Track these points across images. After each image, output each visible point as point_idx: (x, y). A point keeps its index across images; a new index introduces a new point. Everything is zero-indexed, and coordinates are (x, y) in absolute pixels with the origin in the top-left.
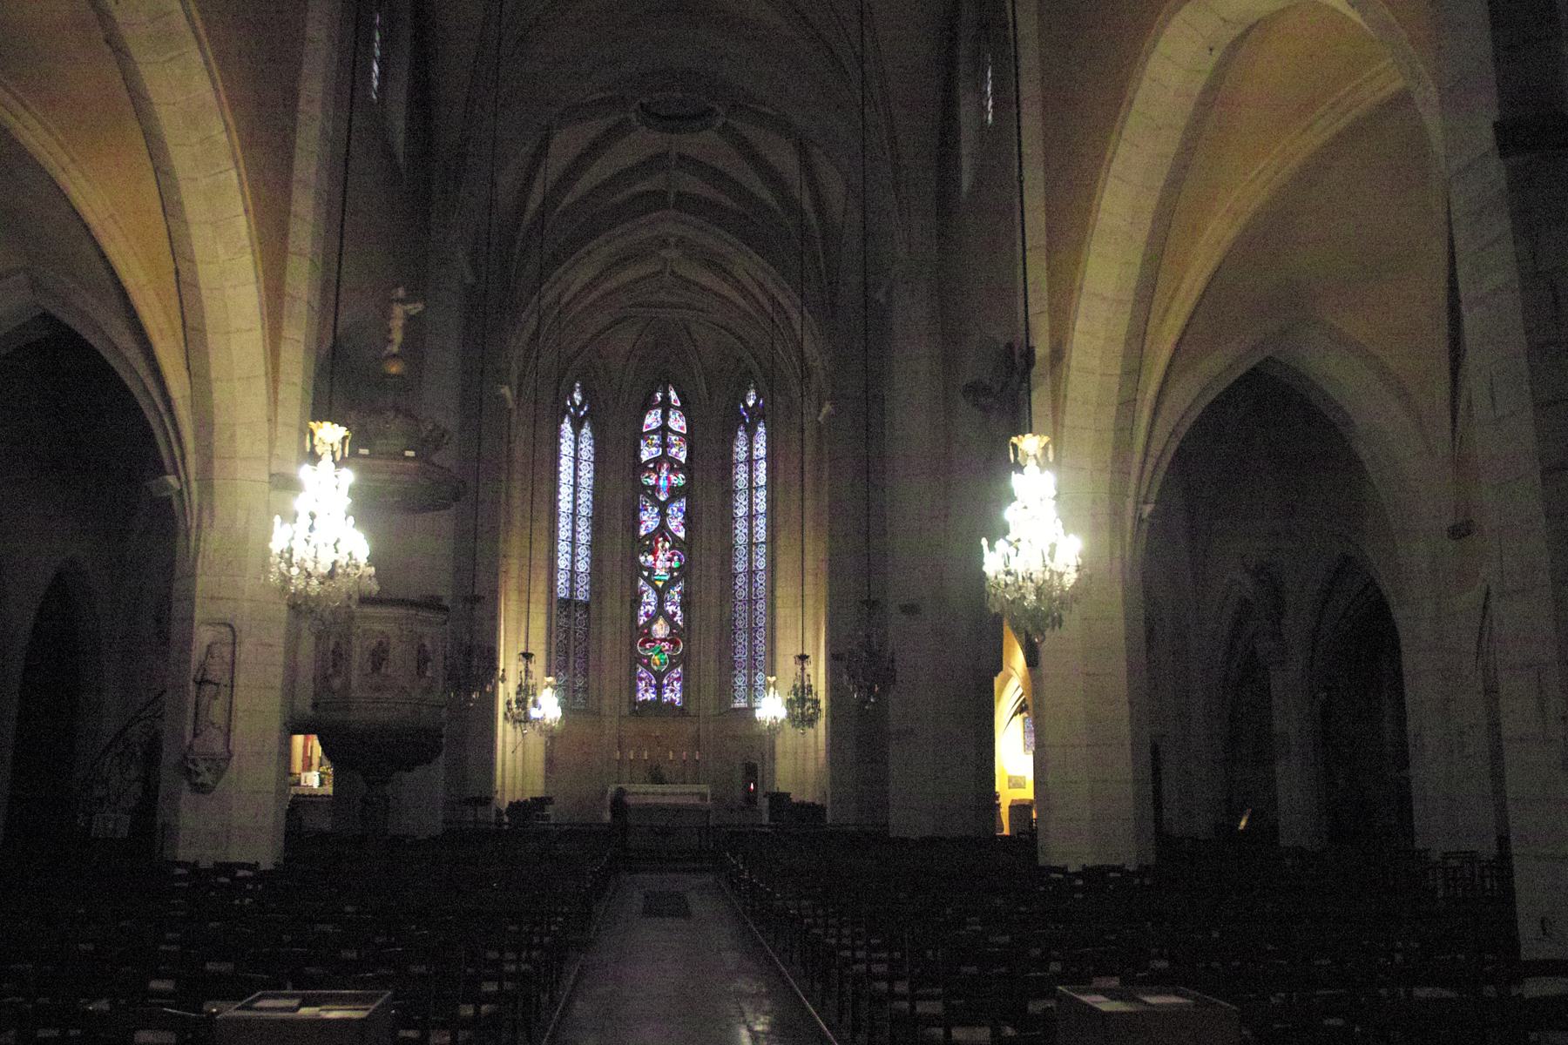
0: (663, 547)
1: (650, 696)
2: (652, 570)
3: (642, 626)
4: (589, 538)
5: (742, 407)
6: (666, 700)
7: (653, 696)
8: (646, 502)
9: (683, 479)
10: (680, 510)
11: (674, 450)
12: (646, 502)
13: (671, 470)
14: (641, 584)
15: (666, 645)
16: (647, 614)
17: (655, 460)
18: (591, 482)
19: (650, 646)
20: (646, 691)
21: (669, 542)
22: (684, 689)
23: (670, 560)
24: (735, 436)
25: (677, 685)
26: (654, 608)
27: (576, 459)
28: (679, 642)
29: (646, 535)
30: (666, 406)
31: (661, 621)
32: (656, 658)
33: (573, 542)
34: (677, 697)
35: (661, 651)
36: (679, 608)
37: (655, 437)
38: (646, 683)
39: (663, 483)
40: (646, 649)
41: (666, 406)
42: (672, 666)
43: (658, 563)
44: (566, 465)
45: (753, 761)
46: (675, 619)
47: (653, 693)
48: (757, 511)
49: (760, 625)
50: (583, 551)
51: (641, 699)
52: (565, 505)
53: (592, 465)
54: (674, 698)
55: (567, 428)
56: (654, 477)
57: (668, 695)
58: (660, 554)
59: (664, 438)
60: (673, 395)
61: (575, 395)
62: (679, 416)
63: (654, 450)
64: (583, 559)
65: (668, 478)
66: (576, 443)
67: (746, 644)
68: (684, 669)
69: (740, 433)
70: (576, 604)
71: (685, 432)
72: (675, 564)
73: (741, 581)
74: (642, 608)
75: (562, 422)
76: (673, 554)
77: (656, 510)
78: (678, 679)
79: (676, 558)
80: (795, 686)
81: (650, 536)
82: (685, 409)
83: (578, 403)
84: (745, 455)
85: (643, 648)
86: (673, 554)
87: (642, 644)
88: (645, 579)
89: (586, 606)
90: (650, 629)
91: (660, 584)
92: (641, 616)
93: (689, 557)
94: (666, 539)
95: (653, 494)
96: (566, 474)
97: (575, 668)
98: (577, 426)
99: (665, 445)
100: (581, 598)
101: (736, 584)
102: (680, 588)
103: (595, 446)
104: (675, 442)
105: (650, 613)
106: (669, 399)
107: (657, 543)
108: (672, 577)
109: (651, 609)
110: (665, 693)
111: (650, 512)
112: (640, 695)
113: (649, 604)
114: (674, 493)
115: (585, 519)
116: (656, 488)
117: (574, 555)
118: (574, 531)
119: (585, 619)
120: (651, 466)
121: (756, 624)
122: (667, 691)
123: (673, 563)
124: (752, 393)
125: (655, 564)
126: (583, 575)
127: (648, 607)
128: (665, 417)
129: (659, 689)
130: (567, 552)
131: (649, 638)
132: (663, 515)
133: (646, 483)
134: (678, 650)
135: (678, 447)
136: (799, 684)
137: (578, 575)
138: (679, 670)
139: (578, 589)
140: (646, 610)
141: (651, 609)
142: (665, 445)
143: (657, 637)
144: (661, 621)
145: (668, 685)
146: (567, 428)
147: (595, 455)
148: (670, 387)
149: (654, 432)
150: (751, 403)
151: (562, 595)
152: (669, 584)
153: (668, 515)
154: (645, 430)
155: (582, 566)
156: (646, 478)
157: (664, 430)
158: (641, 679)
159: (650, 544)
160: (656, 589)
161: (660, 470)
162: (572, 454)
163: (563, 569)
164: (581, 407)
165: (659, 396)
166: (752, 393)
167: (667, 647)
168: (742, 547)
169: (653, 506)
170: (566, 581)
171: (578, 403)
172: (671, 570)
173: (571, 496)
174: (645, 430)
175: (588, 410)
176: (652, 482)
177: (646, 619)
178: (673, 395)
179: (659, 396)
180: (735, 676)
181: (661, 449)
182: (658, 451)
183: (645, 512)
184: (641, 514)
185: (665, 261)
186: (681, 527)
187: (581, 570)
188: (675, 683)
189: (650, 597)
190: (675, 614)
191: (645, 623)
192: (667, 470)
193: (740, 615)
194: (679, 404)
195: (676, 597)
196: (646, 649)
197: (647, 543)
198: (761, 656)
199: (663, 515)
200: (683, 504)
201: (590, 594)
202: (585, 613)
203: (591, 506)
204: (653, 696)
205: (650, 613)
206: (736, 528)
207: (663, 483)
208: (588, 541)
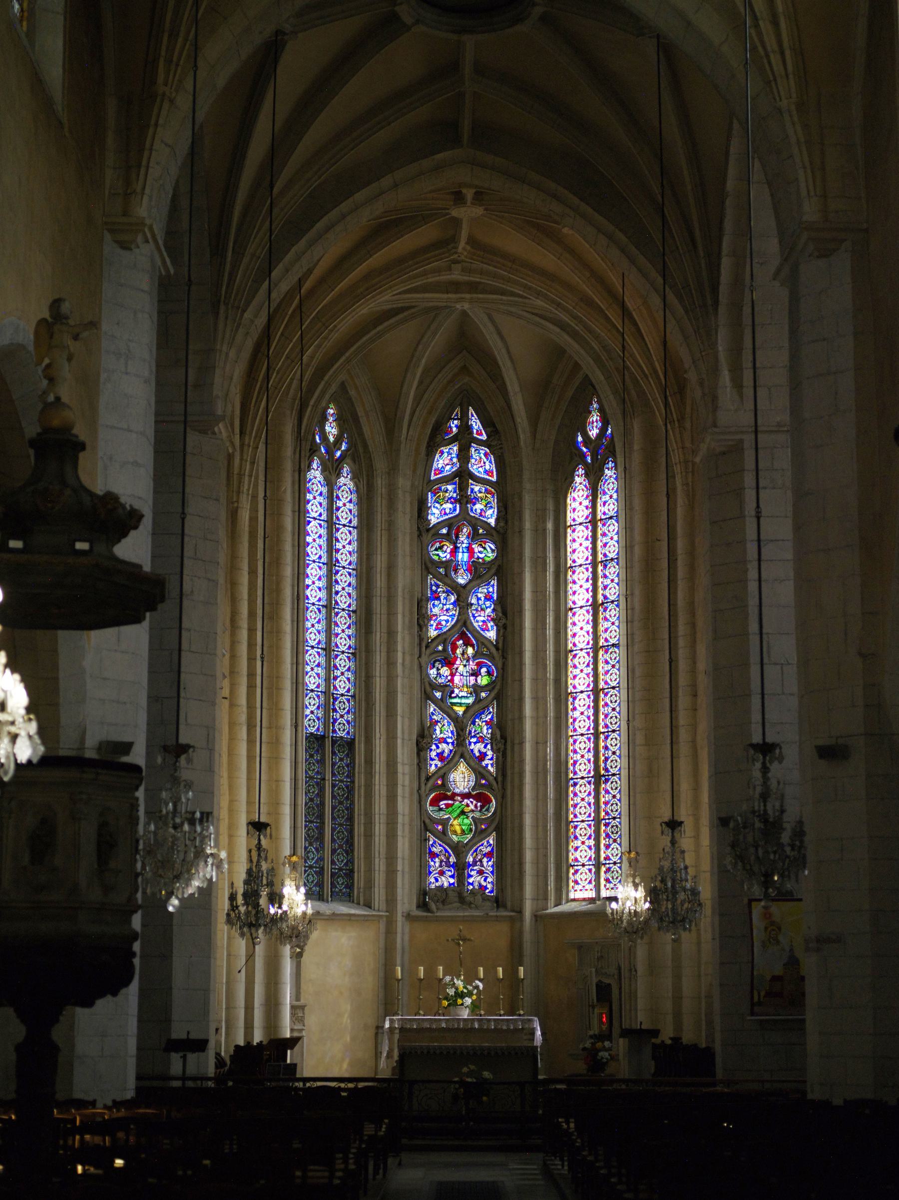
0: (463, 654)
1: (446, 881)
2: (448, 689)
3: (434, 774)
4: (352, 642)
5: (580, 439)
6: (471, 887)
7: (452, 881)
8: (438, 586)
9: (493, 551)
10: (488, 598)
11: (478, 507)
12: (438, 586)
13: (474, 536)
14: (432, 710)
15: (472, 804)
16: (440, 756)
17: (449, 523)
18: (354, 558)
19: (448, 806)
20: (442, 873)
21: (473, 646)
22: (500, 870)
23: (475, 674)
24: (567, 483)
25: (488, 865)
26: (451, 747)
27: (331, 525)
28: (492, 801)
29: (439, 635)
30: (465, 439)
31: (462, 767)
32: (455, 822)
33: (328, 650)
34: (489, 883)
35: (463, 813)
36: (489, 747)
37: (450, 488)
38: (441, 861)
39: (463, 557)
40: (441, 809)
41: (465, 439)
42: (479, 834)
43: (457, 679)
44: (315, 531)
45: (607, 981)
46: (484, 763)
47: (451, 876)
48: (605, 597)
49: (612, 771)
50: (342, 662)
51: (433, 886)
52: (315, 594)
53: (355, 533)
54: (484, 884)
55: (315, 474)
56: (449, 547)
57: (475, 879)
58: (459, 665)
59: (462, 488)
60: (476, 424)
61: (328, 428)
62: (486, 455)
63: (448, 506)
64: (342, 674)
65: (470, 550)
66: (331, 498)
67: (592, 801)
68: (500, 840)
69: (577, 479)
70: (334, 742)
71: (494, 479)
72: (484, 680)
73: (582, 704)
74: (434, 747)
75: (309, 467)
76: (480, 665)
77: (453, 598)
78: (489, 855)
79: (484, 670)
80: (661, 869)
81: (442, 638)
82: (494, 445)
83: (332, 439)
84: (587, 512)
85: (436, 808)
86: (480, 665)
87: (435, 802)
88: (435, 701)
89: (350, 744)
90: (444, 777)
91: (460, 710)
92: (432, 759)
93: (503, 670)
94: (467, 643)
95: (447, 575)
96: (315, 549)
97: (333, 840)
98: (332, 471)
99: (464, 499)
100: (341, 734)
101: (575, 709)
102: (489, 717)
103: (360, 504)
104: (479, 495)
105: (445, 755)
106: (470, 428)
107: (454, 648)
108: (478, 700)
109: (446, 748)
110: (470, 876)
111: (443, 601)
112: (433, 880)
113: (444, 741)
114: (478, 570)
115: (344, 614)
116: (451, 566)
117: (330, 668)
118: (329, 633)
119: (347, 766)
120: (444, 531)
121: (607, 770)
122: (473, 873)
123: (479, 678)
124: (595, 417)
125: (452, 681)
126: (344, 699)
127: (443, 746)
128: (464, 456)
129: (461, 869)
130: (318, 665)
131: (444, 794)
132: (462, 604)
133: (436, 558)
134: (488, 810)
135: (484, 502)
136: (666, 864)
137: (335, 699)
138: (491, 842)
139: (335, 720)
140: (439, 751)
141: (446, 748)
142: (464, 499)
143: (457, 791)
144: (462, 767)
146: (315, 474)
147: (360, 516)
148: (471, 410)
149: (448, 480)
150: (594, 433)
151: (312, 730)
152: (475, 711)
153: (472, 604)
154: (433, 478)
155: (342, 685)
156: (436, 550)
157: (463, 476)
158: (433, 855)
159: (445, 650)
160: (455, 719)
161: (457, 537)
162: (324, 517)
163: (312, 691)
164: (339, 440)
165: (454, 425)
166: (595, 417)
167: (472, 807)
168: (583, 653)
169: (448, 592)
170: (318, 708)
171: (332, 439)
172: (476, 689)
173: (324, 580)
174: (433, 478)
175: (347, 450)
176: (445, 555)
177: (439, 764)
178: (476, 424)
179: (454, 425)
180: (576, 849)
181: (458, 506)
182: (455, 510)
183: (436, 602)
184: (430, 605)
185: (456, 223)
186: (490, 624)
187: (342, 691)
188: (485, 860)
189: (444, 730)
190: (483, 756)
191: (439, 769)
192: (468, 537)
193: (583, 756)
194: (484, 437)
195: (485, 731)
196: (441, 809)
197: (440, 648)
198: (614, 818)
199: (462, 604)
200: (493, 588)
201: (354, 727)
202: (347, 755)
203: (354, 594)
204: (452, 881)
205: (445, 755)
206: (574, 624)
207: (463, 557)
208: (350, 647)
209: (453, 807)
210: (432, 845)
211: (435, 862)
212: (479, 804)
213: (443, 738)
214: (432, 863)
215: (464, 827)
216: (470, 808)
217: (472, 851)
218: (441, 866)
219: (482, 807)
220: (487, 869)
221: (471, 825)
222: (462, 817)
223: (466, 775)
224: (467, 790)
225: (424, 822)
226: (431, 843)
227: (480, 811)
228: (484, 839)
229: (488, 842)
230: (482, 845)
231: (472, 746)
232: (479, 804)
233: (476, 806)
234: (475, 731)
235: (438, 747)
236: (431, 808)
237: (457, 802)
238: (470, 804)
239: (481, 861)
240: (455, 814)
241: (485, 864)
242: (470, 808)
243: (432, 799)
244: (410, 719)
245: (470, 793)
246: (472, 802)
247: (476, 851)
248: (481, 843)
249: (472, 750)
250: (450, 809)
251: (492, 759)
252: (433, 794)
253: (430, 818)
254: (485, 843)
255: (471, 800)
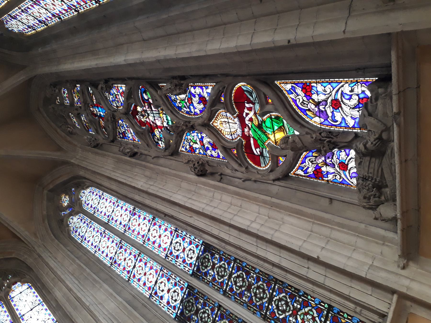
19: (257, 146)
28: (240, 87)
32: (272, 137)
35: (260, 127)
38: (326, 164)
40: (262, 153)
54: (354, 101)
85: (262, 160)
122: (338, 116)
138: (289, 87)
143: (239, 132)
145: (322, 114)
196: (262, 153)
202: (213, 255)
209: (257, 138)
210: (306, 172)
211: (328, 173)
212: (247, 105)
213: (200, 141)
214: (330, 177)
215: (276, 128)
216: (254, 117)
217: (304, 117)
218: (333, 166)
219: (249, 102)
220: (330, 94)
221: (270, 117)
222: (265, 128)
223: (223, 120)
224: (236, 120)
225: (274, 180)
226: (302, 173)
227: (254, 104)
228: (286, 98)
229: (290, 92)
230: (295, 101)
231: (197, 111)
232: (247, 105)
233: (250, 109)
234: (185, 107)
235: (208, 148)
236: (263, 165)
237: (251, 133)
238: (249, 116)
239: (317, 104)
240: (265, 138)
241: (322, 97)
242: (254, 117)
243: (254, 163)
244: (183, 179)
245: (238, 116)
246: (247, 114)
247: (304, 111)
248: (293, 103)
249: (201, 112)
250: (259, 142)
251: (201, 87)
252: (248, 160)
253: (272, 170)
254: (292, 96)
255: (244, 115)
